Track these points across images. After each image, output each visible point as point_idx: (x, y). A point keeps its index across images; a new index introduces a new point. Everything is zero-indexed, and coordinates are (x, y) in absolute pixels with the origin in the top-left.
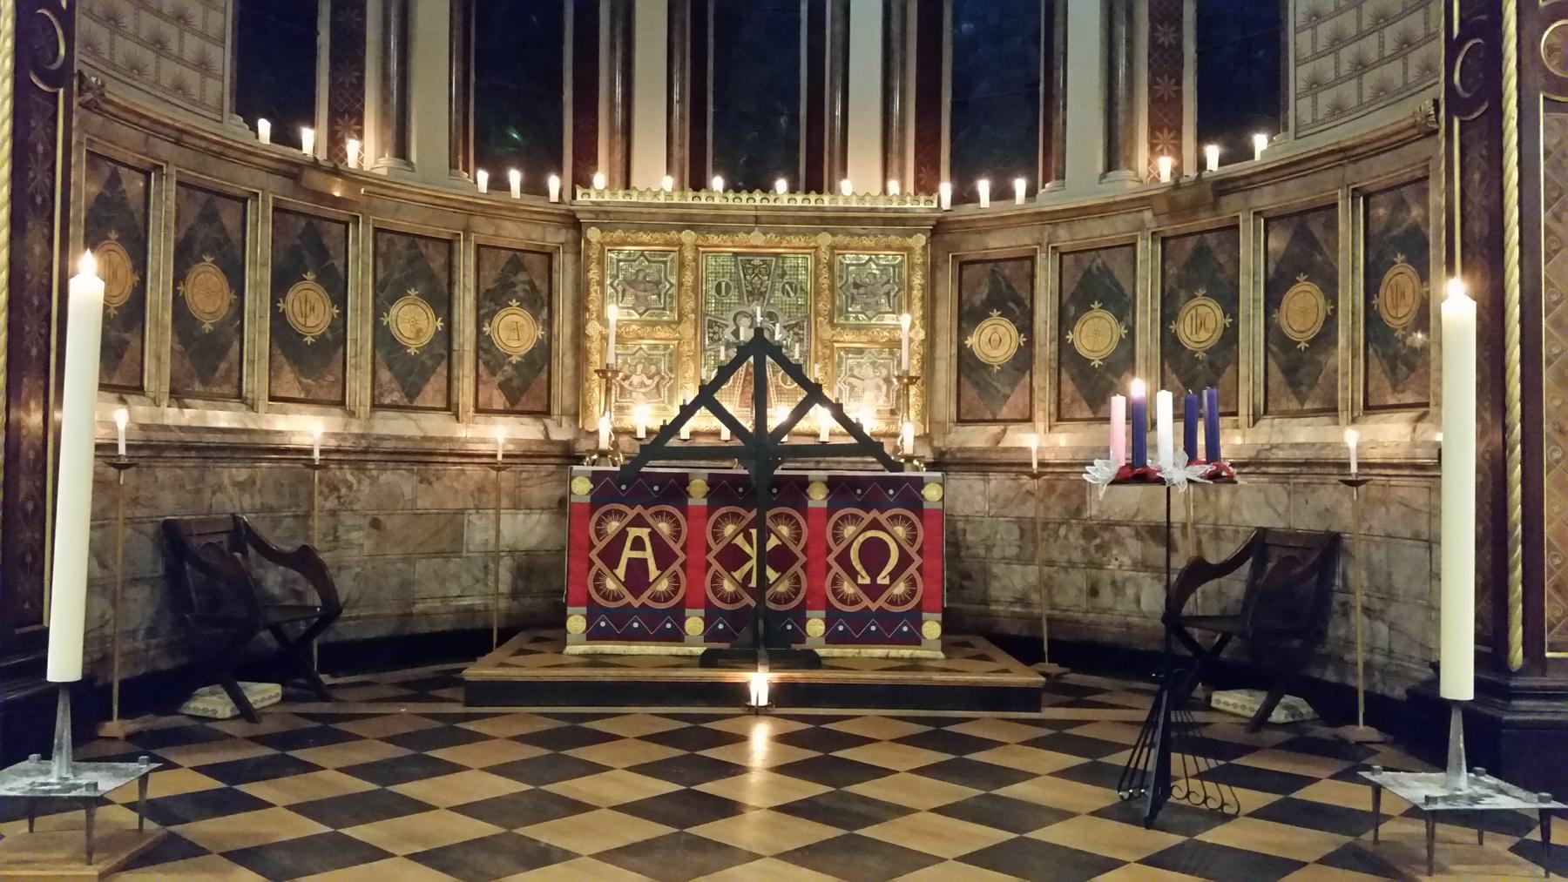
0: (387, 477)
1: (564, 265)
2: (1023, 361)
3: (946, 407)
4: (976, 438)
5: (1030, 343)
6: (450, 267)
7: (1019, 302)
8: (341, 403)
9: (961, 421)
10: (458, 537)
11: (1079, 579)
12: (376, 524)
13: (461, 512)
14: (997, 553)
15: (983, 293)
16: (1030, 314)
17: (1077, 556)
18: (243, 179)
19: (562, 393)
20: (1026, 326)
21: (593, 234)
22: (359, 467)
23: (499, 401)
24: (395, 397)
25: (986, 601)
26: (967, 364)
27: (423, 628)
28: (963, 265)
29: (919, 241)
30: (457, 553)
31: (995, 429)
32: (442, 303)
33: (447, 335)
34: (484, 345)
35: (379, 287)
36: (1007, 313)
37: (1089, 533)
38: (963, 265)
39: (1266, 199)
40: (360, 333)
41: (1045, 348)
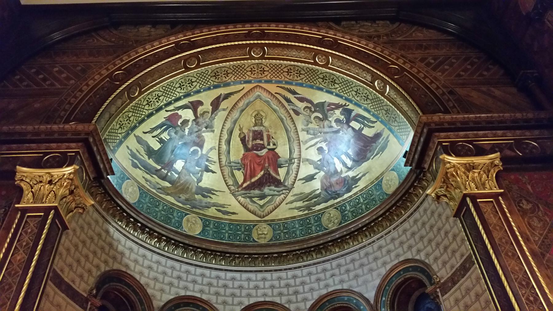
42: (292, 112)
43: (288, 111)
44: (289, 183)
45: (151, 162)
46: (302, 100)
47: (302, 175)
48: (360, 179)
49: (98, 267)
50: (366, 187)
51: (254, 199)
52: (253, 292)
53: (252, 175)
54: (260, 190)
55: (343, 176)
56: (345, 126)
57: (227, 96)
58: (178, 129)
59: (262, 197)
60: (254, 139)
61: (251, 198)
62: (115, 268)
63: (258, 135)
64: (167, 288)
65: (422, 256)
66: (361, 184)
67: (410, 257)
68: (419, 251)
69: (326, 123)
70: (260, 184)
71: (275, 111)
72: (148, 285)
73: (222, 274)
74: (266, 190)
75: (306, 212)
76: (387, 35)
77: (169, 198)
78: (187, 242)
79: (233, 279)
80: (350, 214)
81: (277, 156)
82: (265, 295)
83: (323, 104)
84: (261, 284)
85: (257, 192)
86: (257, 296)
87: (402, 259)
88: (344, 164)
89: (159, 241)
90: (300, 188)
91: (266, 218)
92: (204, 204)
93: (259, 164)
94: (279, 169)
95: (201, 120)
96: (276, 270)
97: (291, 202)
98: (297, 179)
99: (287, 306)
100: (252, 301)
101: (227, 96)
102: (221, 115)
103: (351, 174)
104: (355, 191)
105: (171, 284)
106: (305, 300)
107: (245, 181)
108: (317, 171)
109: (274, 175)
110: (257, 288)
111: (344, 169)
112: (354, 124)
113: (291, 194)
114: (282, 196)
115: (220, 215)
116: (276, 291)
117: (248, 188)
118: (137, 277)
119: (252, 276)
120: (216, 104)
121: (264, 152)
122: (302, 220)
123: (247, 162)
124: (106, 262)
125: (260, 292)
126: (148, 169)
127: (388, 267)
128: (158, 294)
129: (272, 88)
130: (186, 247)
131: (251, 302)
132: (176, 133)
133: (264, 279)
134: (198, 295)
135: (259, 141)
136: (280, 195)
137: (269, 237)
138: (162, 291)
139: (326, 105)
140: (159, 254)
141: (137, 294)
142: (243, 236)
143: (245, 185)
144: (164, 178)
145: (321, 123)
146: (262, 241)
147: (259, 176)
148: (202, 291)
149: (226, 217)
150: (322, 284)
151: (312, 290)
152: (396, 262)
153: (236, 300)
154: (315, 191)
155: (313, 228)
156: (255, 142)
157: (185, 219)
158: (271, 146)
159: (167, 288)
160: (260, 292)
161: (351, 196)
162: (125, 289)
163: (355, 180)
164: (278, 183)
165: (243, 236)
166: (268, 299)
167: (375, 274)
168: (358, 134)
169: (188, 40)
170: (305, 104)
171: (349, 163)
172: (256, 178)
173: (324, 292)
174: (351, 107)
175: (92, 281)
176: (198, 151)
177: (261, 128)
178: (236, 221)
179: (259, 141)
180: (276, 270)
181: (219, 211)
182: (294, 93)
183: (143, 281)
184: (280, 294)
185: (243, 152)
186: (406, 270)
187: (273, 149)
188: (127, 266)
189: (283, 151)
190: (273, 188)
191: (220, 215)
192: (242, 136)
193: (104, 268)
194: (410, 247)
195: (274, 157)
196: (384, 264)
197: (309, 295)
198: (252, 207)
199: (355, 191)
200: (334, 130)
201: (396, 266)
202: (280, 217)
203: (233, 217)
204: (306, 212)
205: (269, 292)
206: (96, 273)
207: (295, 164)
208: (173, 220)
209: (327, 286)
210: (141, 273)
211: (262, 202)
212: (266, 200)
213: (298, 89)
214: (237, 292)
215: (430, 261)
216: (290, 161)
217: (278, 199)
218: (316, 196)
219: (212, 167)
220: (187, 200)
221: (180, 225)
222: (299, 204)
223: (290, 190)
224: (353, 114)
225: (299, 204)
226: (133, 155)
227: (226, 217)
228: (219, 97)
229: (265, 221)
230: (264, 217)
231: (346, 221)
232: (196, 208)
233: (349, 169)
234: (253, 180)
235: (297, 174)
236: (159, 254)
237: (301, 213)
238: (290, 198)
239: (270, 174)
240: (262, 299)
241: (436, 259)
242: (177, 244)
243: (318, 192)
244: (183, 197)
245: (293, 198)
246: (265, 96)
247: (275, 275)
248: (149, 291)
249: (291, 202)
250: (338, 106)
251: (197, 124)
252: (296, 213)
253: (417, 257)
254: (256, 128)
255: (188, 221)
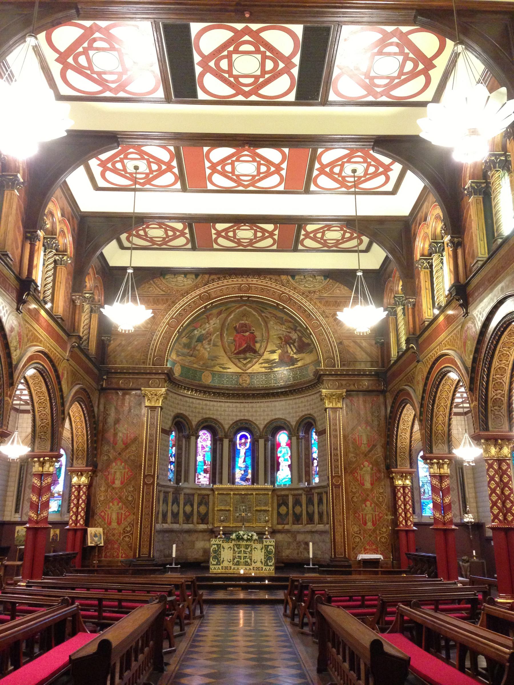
0: (184, 535)
1: (211, 497)
2: (287, 514)
3: (275, 522)
4: (280, 527)
5: (288, 511)
6: (194, 499)
7: (287, 503)
8: (178, 523)
9: (278, 524)
10: (194, 546)
11: (296, 552)
12: (183, 543)
13: (194, 541)
14: (284, 548)
15: (281, 502)
16: (288, 505)
17: (296, 548)
18: (169, 490)
19: (210, 519)
20: (288, 508)
21: (216, 493)
22: (181, 534)
23: (200, 521)
24: (186, 522)
25: (282, 557)
26: (279, 514)
27: (189, 561)
28: (278, 496)
29: (270, 493)
30: (193, 548)
31: (283, 526)
32: (192, 505)
33: (193, 511)
34: (198, 512)
35: (184, 504)
36: (285, 505)
37: (297, 544)
38: (278, 496)
39: (317, 491)
40: (181, 512)
41: (291, 512)
42: (265, 318)
43: (262, 316)
44: (261, 352)
45: (186, 351)
46: (270, 313)
47: (268, 349)
48: (299, 361)
49: (171, 415)
50: (301, 366)
51: (241, 360)
52: (239, 414)
53: (240, 346)
54: (244, 354)
55: (291, 355)
56: (294, 332)
57: (226, 310)
58: (199, 329)
59: (245, 359)
60: (242, 327)
61: (239, 359)
62: (176, 412)
63: (245, 325)
64: (197, 415)
65: (315, 415)
66: (299, 364)
67: (312, 413)
68: (315, 412)
69: (284, 327)
70: (244, 351)
71: (254, 315)
72: (189, 415)
73: (222, 404)
74: (248, 355)
75: (269, 370)
76: (319, 291)
77: (195, 366)
78: (205, 390)
79: (229, 407)
80: (292, 379)
81: (255, 337)
82: (244, 415)
83: (282, 318)
84: (243, 410)
85: (242, 356)
86: (240, 416)
87: (309, 412)
88: (292, 350)
89: (192, 391)
90: (266, 355)
91: (248, 371)
92: (212, 365)
93: (244, 340)
94: (256, 344)
95: (211, 321)
96: (251, 402)
97: (262, 363)
98: (267, 350)
99: (255, 422)
100: (238, 418)
101: (226, 310)
102: (223, 315)
103: (295, 356)
104: (296, 366)
105: (199, 413)
106: (264, 419)
107: (235, 350)
108: (277, 349)
109: (253, 347)
110: (240, 411)
111: (292, 353)
112: (298, 332)
113: (262, 359)
114: (257, 359)
115: (221, 370)
116: (250, 414)
117: (238, 353)
118: (185, 413)
119: (238, 405)
120: (220, 313)
121: (247, 334)
122: (266, 375)
123: (237, 339)
124: (173, 411)
125: (242, 414)
126: (183, 355)
127: (303, 414)
128: (194, 418)
129: (254, 305)
130: (205, 392)
131: (238, 419)
132: (197, 331)
133: (244, 407)
134: (212, 416)
135: (244, 328)
136: (255, 358)
137: (248, 382)
138: (195, 416)
139: (284, 318)
140: (192, 398)
141: (185, 420)
142: (234, 382)
143: (235, 352)
144: (191, 356)
145: (281, 326)
146: (245, 385)
147: (244, 347)
148: (213, 414)
149: (225, 371)
150: (273, 413)
151: (268, 415)
152: (306, 413)
153: (230, 418)
154: (275, 359)
155: (272, 381)
156: (242, 329)
157: (203, 375)
158: (252, 331)
159: (197, 415)
160: (242, 414)
161: (293, 368)
162: (181, 420)
163: (297, 360)
164: (255, 352)
165: (234, 382)
166: (246, 418)
167: (298, 414)
168: (300, 338)
169: (205, 292)
170: (272, 315)
171: (295, 351)
172: (242, 348)
173: (274, 417)
174: (297, 325)
175: (170, 423)
176: (209, 337)
177: (247, 322)
178: (230, 372)
179: (244, 328)
180: (251, 402)
181: (221, 367)
182: (266, 309)
183: (187, 414)
184: (252, 415)
185: (235, 334)
186: (310, 418)
187: (253, 333)
188: (180, 409)
189: (257, 334)
190: (252, 354)
191: (221, 370)
192: (235, 325)
193: (173, 414)
194: (313, 408)
195: (253, 338)
196: (302, 411)
197: (266, 417)
198: (239, 365)
199: (296, 366)
200: (288, 331)
201: (306, 415)
202: (255, 372)
203: (229, 370)
204: (269, 370)
205: (247, 414)
206: (171, 418)
207: (264, 344)
208: (197, 377)
209: (275, 414)
210: (186, 410)
211: (245, 362)
212: (248, 360)
213: (267, 308)
214: (231, 413)
215: (317, 419)
216: (262, 341)
217: (255, 360)
218: (275, 363)
219: (218, 344)
220: (204, 364)
221: (200, 379)
222: (266, 365)
223: (261, 356)
224: (298, 328)
225: (266, 365)
226: (177, 352)
227: (225, 371)
228: (221, 311)
229: (247, 373)
230: (246, 370)
231: (290, 381)
232: (208, 367)
233: (295, 353)
234: (240, 349)
235: (266, 348)
236: (192, 398)
237: (266, 371)
238: (261, 361)
239: (250, 346)
240: (243, 418)
241: (319, 420)
242: (200, 391)
243: (277, 360)
244: (201, 363)
245: (263, 361)
246: (248, 309)
247: (250, 405)
248: (190, 418)
249: (262, 363)
250: (290, 322)
251: (209, 324)
252: (263, 370)
253: (314, 415)
254: (243, 322)
255: (204, 375)
